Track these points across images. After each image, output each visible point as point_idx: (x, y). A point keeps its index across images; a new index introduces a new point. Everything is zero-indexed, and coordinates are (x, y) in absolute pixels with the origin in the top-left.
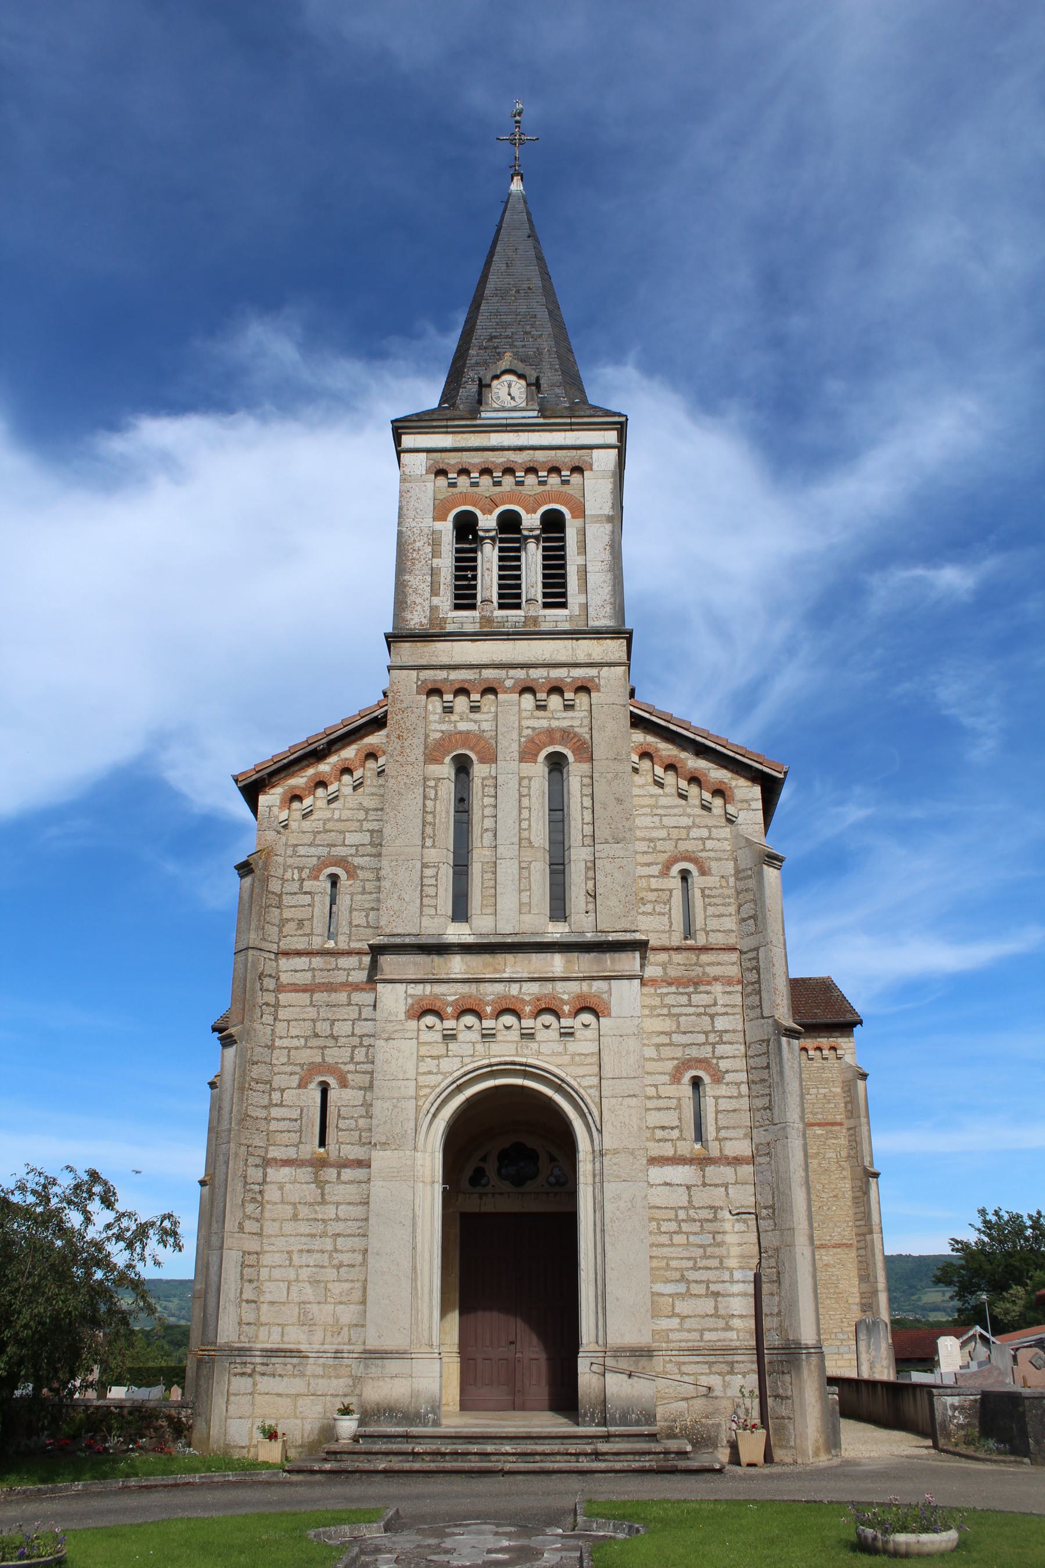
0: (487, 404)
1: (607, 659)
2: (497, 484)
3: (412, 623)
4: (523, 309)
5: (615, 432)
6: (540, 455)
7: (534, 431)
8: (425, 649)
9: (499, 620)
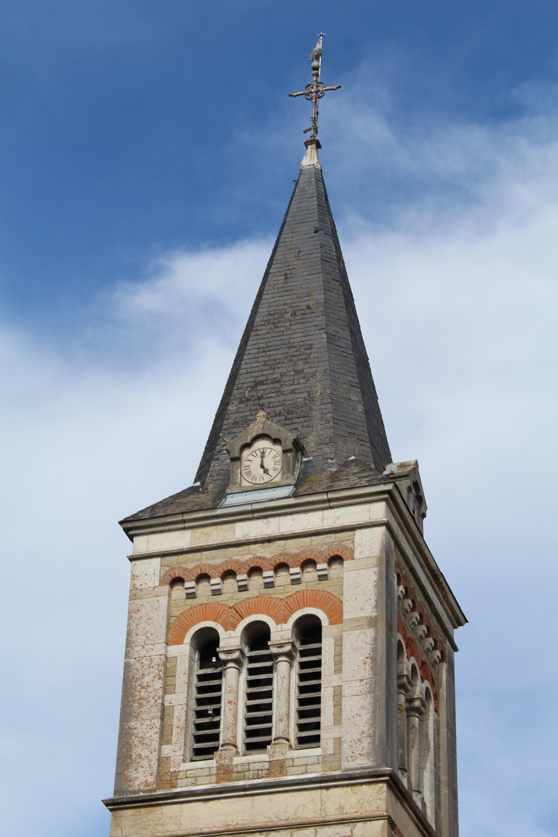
0: (235, 483)
1: (363, 812)
2: (243, 588)
3: (137, 783)
4: (297, 338)
5: (383, 504)
6: (293, 546)
7: (286, 514)
8: (150, 817)
9: (240, 769)
